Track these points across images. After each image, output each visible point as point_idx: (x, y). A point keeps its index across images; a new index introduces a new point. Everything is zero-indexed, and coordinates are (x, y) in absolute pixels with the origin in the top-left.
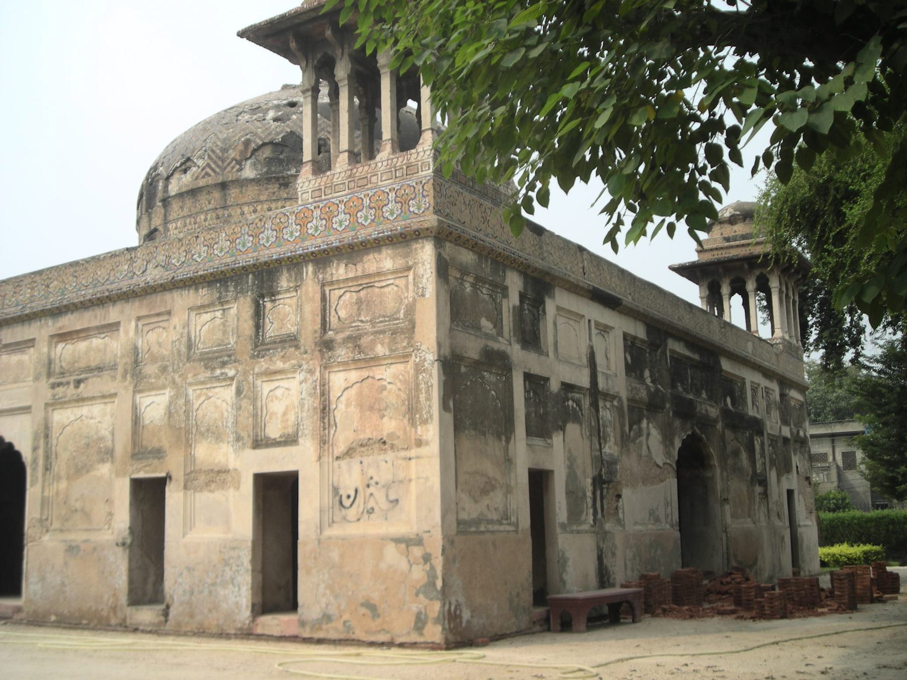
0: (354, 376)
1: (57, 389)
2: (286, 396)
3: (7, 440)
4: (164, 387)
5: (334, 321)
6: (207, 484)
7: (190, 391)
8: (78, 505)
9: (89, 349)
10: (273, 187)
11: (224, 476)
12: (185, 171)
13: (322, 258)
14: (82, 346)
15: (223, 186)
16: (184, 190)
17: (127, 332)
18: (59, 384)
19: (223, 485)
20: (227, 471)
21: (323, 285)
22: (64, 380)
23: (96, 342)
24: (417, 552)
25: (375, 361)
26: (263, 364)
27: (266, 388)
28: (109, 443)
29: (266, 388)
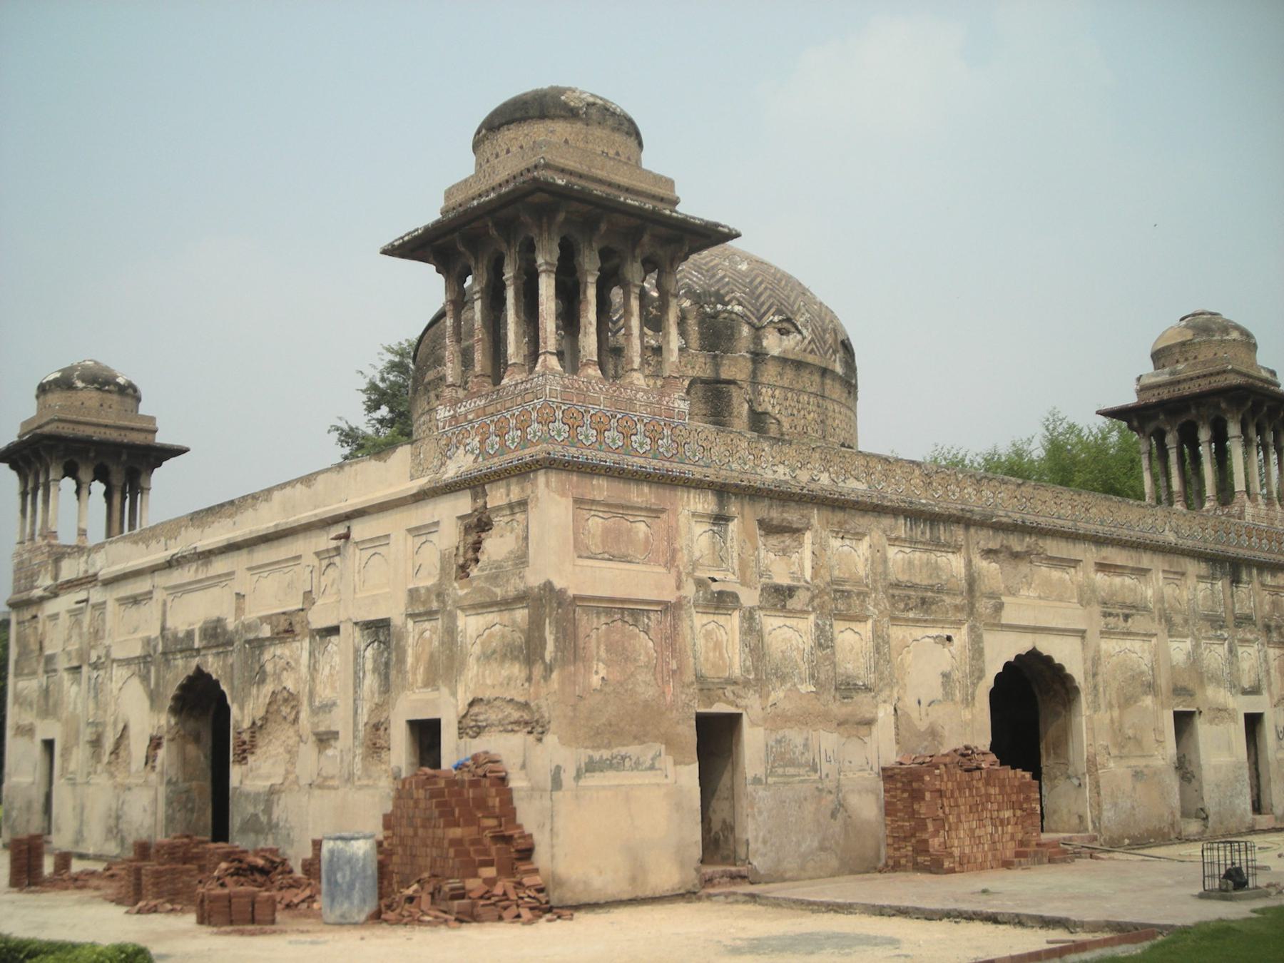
1: (1110, 619)
3: (1057, 661)
4: (1186, 637)
8: (1130, 733)
9: (1123, 586)
11: (1223, 713)
15: (824, 372)
16: (791, 356)
17: (1157, 580)
18: (1110, 615)
23: (1128, 581)
26: (1240, 634)
27: (1240, 650)
28: (1150, 678)
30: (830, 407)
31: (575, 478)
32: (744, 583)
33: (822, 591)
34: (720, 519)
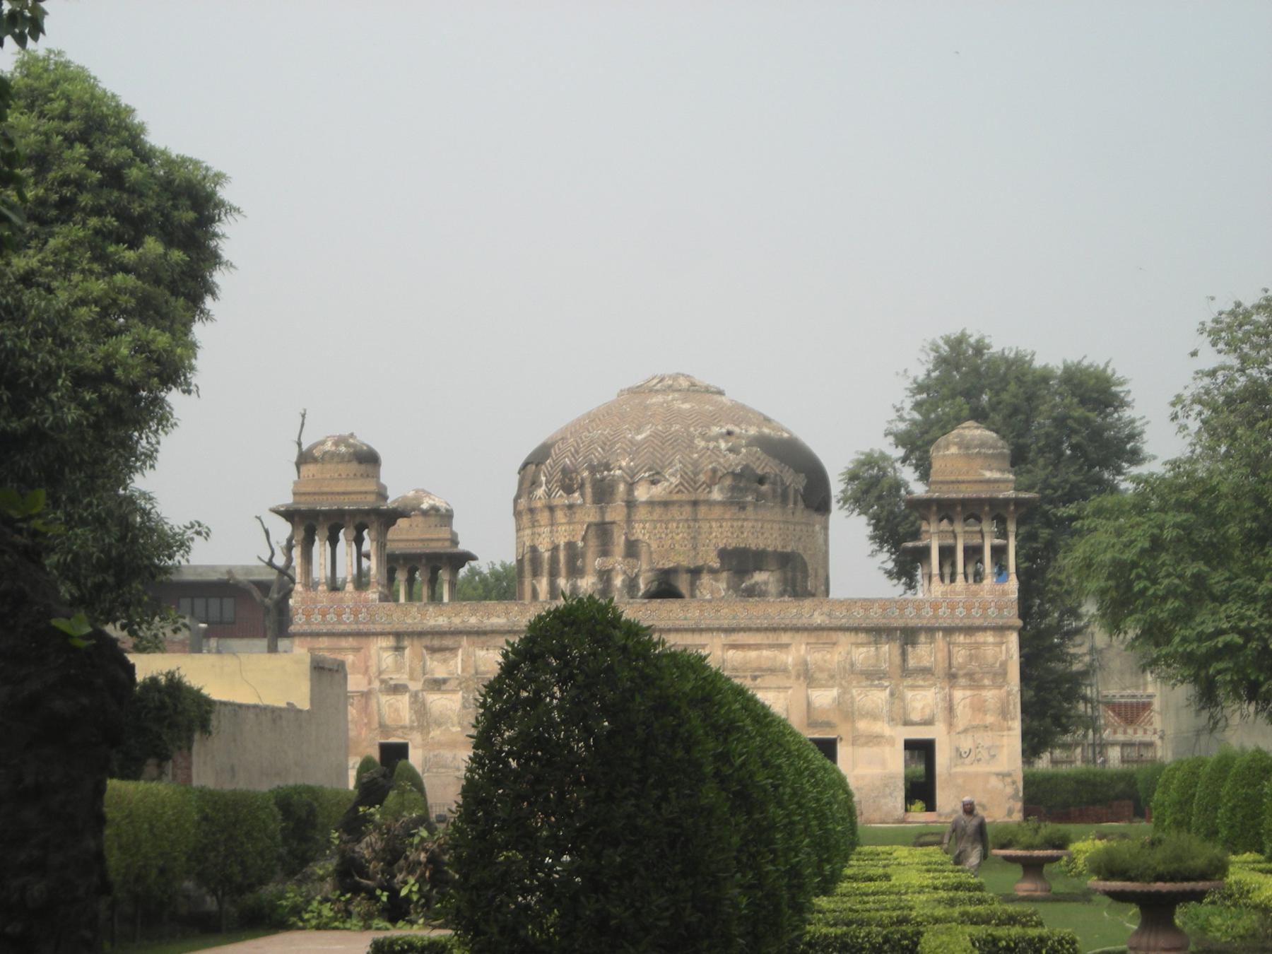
0: (968, 693)
2: (923, 699)
4: (833, 687)
5: (955, 663)
6: (866, 744)
7: (854, 692)
10: (734, 509)
12: (654, 483)
13: (949, 631)
14: (753, 654)
15: (695, 503)
16: (656, 499)
17: (798, 651)
19: (879, 744)
20: (882, 737)
21: (949, 644)
22: (741, 674)
23: (765, 653)
24: (1009, 780)
25: (984, 687)
26: (909, 681)
27: (909, 694)
29: (909, 694)
30: (705, 526)
31: (309, 639)
32: (412, 678)
33: (467, 680)
34: (398, 649)
